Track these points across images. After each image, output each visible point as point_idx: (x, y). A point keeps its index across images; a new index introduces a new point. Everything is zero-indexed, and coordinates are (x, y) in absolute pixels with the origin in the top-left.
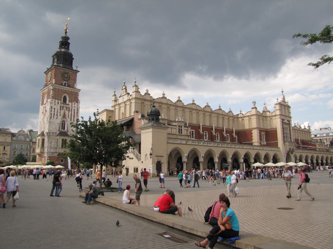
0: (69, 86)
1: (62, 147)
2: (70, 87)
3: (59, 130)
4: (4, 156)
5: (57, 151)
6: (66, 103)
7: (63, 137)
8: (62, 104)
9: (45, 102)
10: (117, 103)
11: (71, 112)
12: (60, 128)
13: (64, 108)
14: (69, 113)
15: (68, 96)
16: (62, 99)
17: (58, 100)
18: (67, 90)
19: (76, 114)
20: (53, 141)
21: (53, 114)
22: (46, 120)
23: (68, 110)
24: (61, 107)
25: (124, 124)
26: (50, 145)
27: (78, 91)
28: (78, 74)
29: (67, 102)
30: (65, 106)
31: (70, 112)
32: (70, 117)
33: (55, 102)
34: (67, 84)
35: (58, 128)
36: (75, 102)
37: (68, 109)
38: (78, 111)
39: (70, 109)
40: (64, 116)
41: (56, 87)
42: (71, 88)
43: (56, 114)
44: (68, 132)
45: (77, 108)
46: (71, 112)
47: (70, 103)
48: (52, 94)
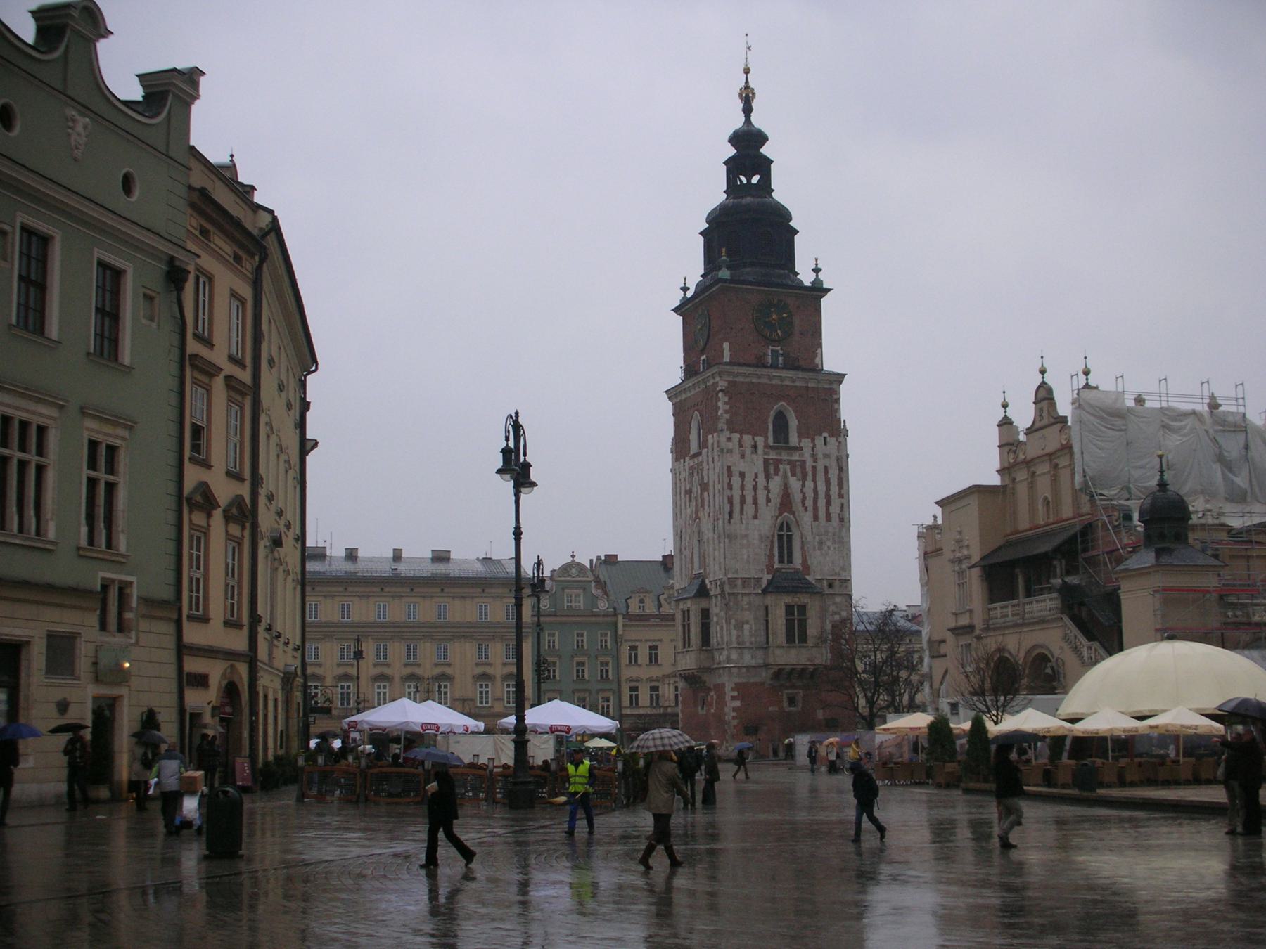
0: (791, 365)
1: (790, 638)
2: (797, 368)
3: (770, 568)
4: (484, 689)
5: (771, 661)
6: (787, 442)
7: (788, 599)
8: (771, 447)
9: (694, 447)
10: (1021, 457)
11: (814, 481)
12: (771, 557)
13: (781, 466)
14: (803, 485)
15: (796, 412)
16: (768, 429)
17: (754, 435)
18: (787, 383)
19: (834, 489)
20: (748, 615)
21: (737, 501)
22: (711, 527)
23: (798, 470)
24: (766, 462)
25: (1057, 550)
26: (738, 637)
27: (831, 383)
28: (825, 302)
29: (794, 440)
30: (784, 456)
31: (809, 484)
32: (809, 503)
33: (741, 446)
34: (785, 355)
35: (764, 560)
36: (826, 435)
37: (799, 469)
38: (844, 475)
39: (809, 469)
40: (786, 503)
41: (741, 379)
42: (800, 374)
43: (749, 499)
44: (809, 574)
45: (839, 459)
46: (814, 481)
47: (806, 443)
48: (726, 412)
